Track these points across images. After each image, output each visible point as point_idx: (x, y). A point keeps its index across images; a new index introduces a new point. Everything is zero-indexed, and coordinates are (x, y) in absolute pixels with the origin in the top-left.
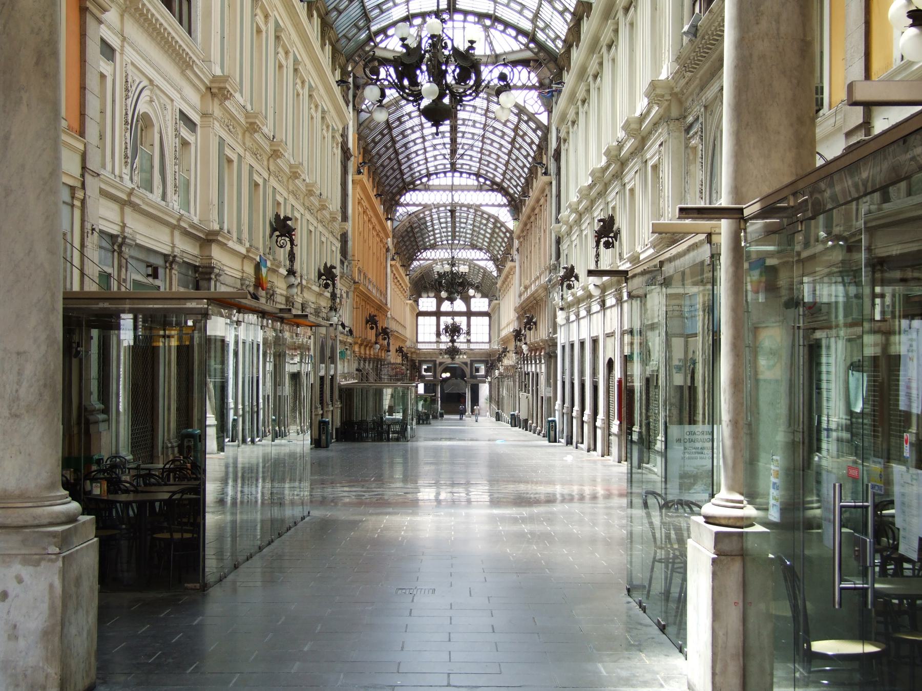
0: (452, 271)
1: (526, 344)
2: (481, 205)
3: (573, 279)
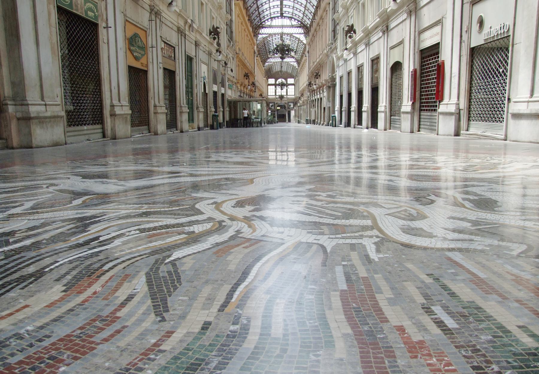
0: (283, 45)
1: (315, 85)
2: (293, 34)
3: (352, 32)
